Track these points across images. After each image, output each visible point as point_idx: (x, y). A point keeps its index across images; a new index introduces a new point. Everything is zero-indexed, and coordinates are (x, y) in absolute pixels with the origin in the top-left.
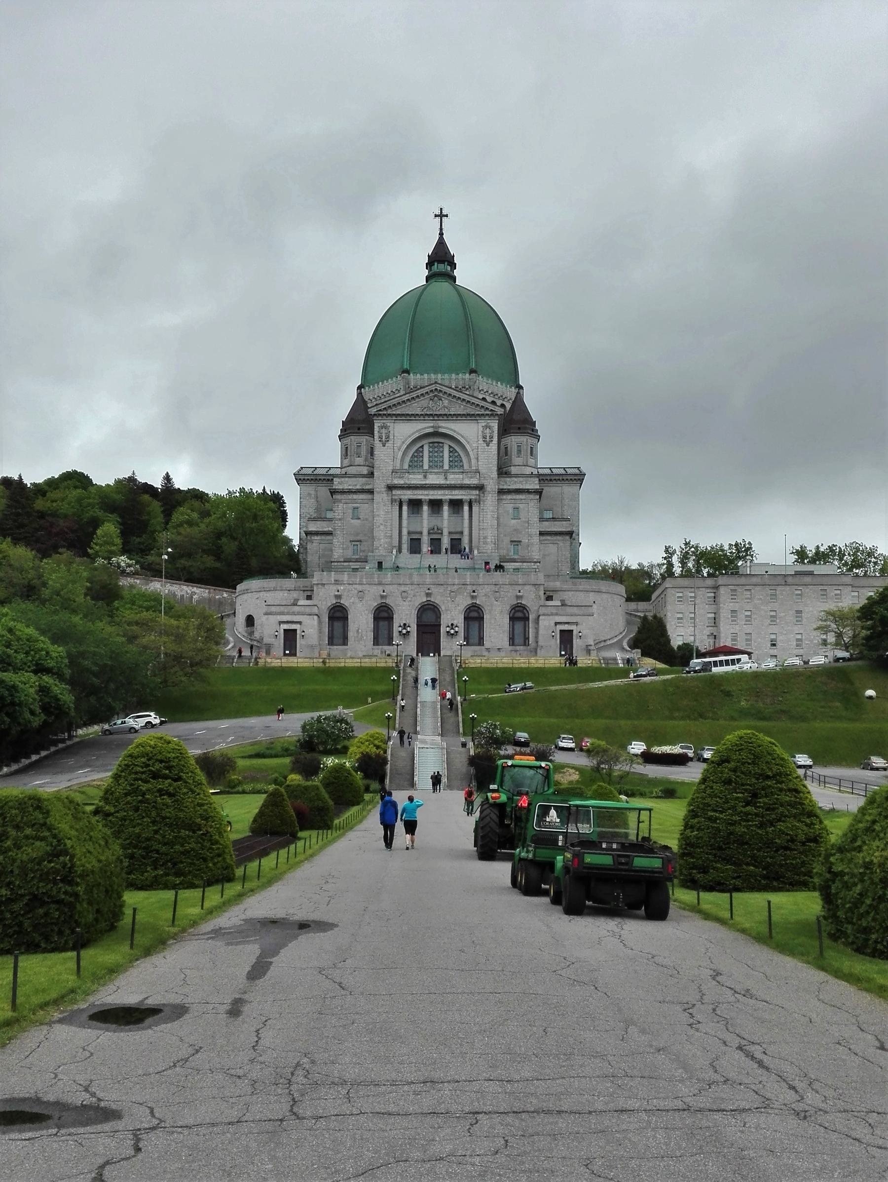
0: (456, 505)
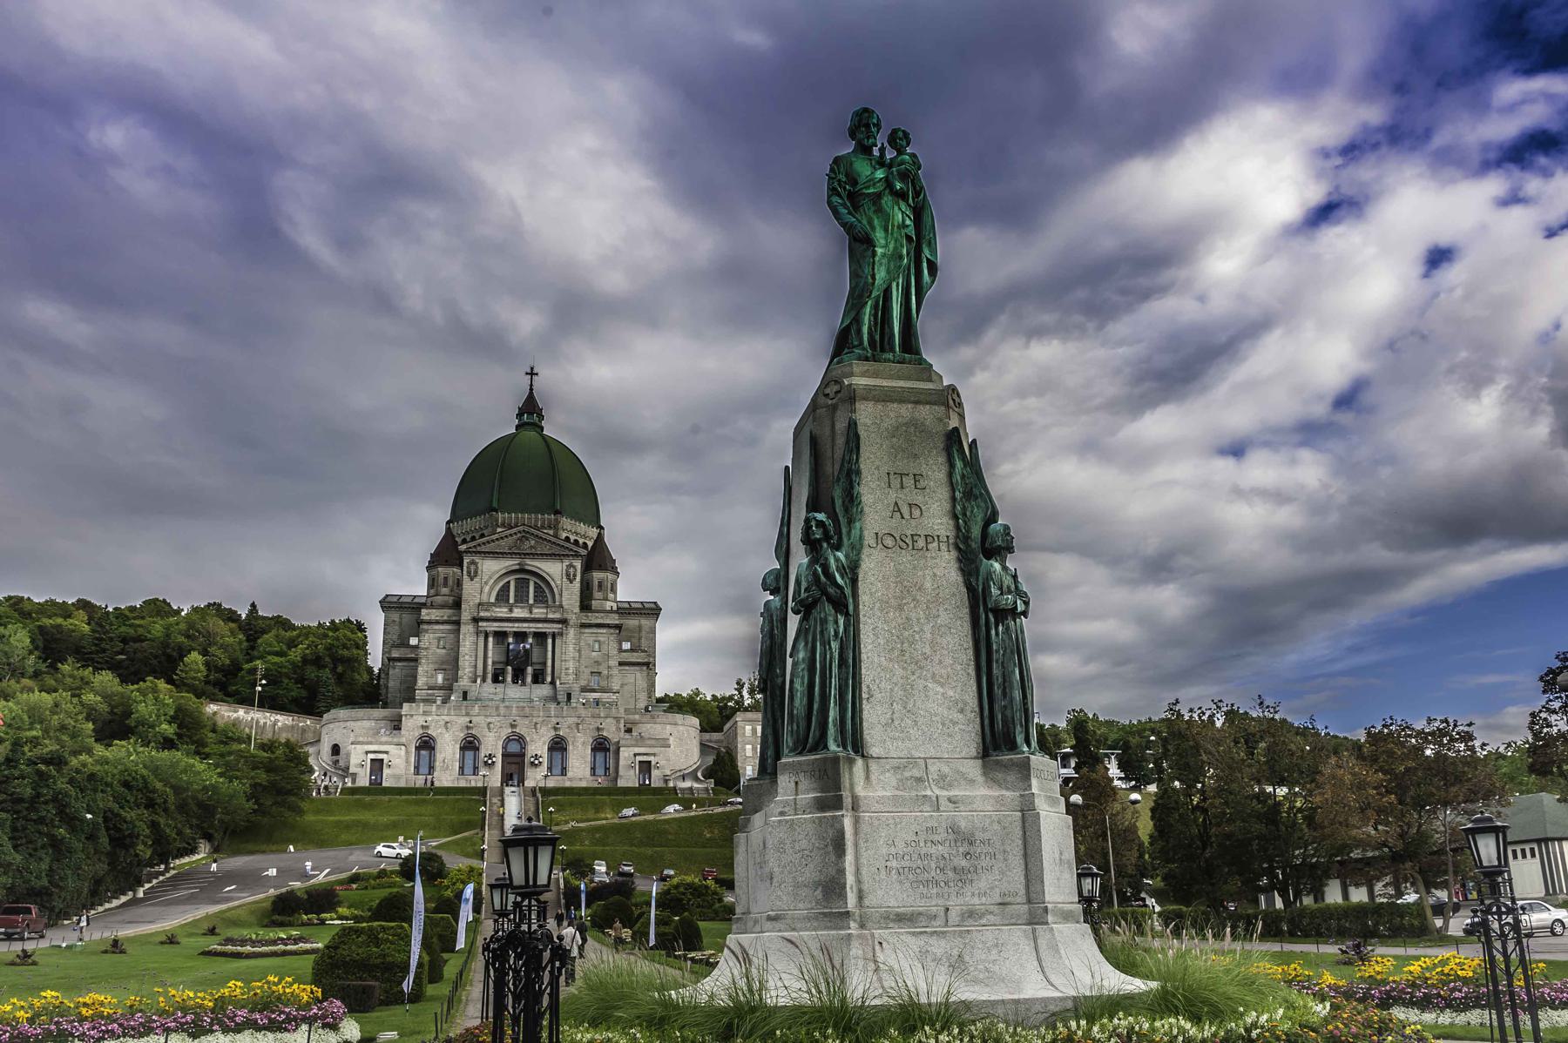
0: (541, 637)
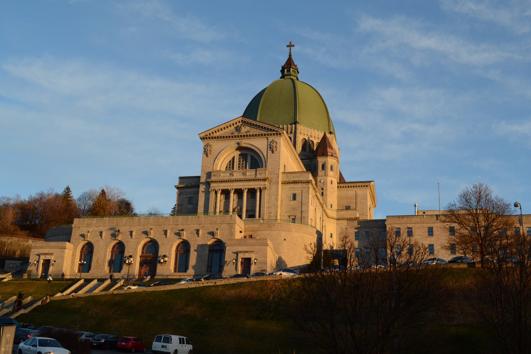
0: (252, 192)
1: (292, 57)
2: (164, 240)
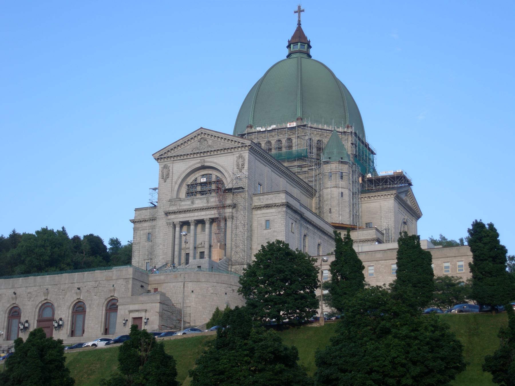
1: (303, 27)
2: (60, 301)
